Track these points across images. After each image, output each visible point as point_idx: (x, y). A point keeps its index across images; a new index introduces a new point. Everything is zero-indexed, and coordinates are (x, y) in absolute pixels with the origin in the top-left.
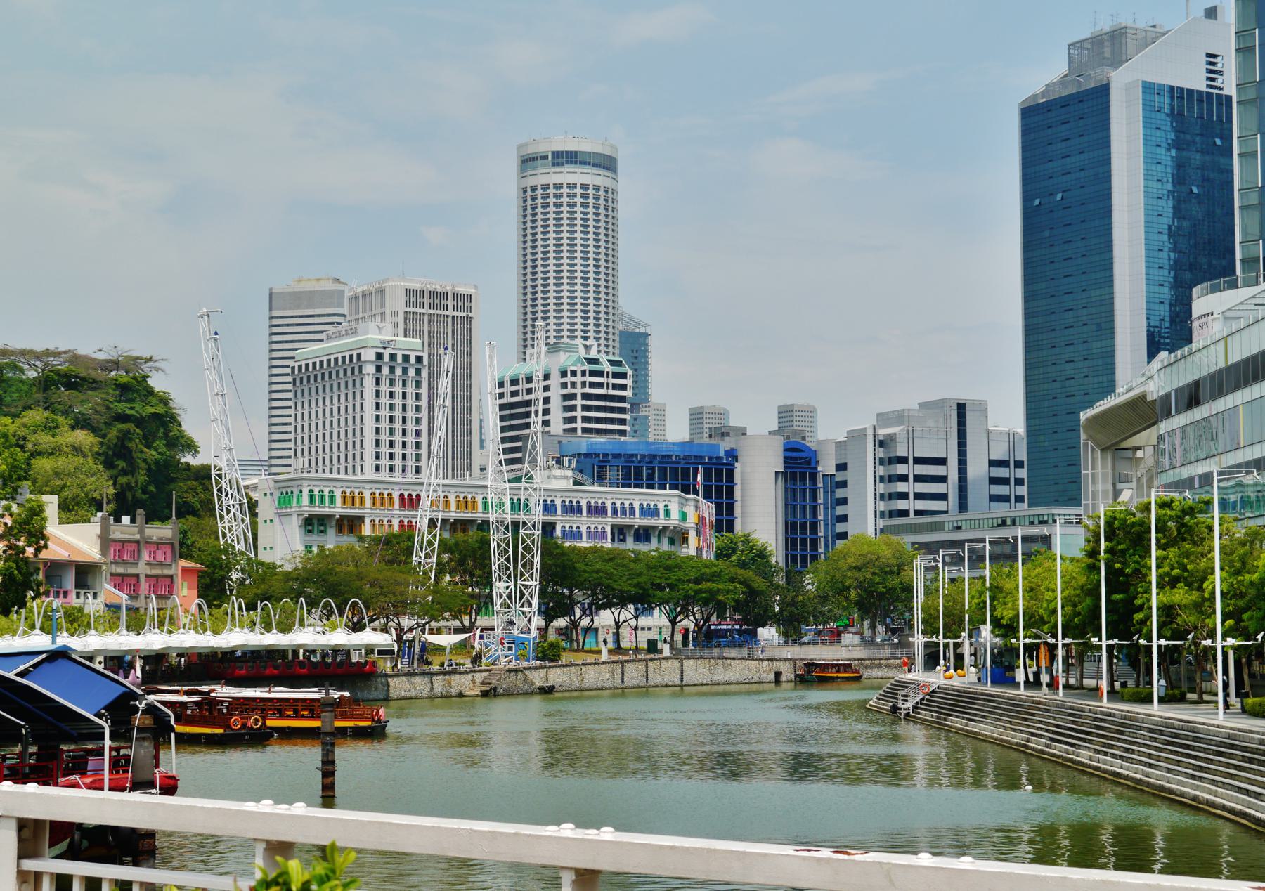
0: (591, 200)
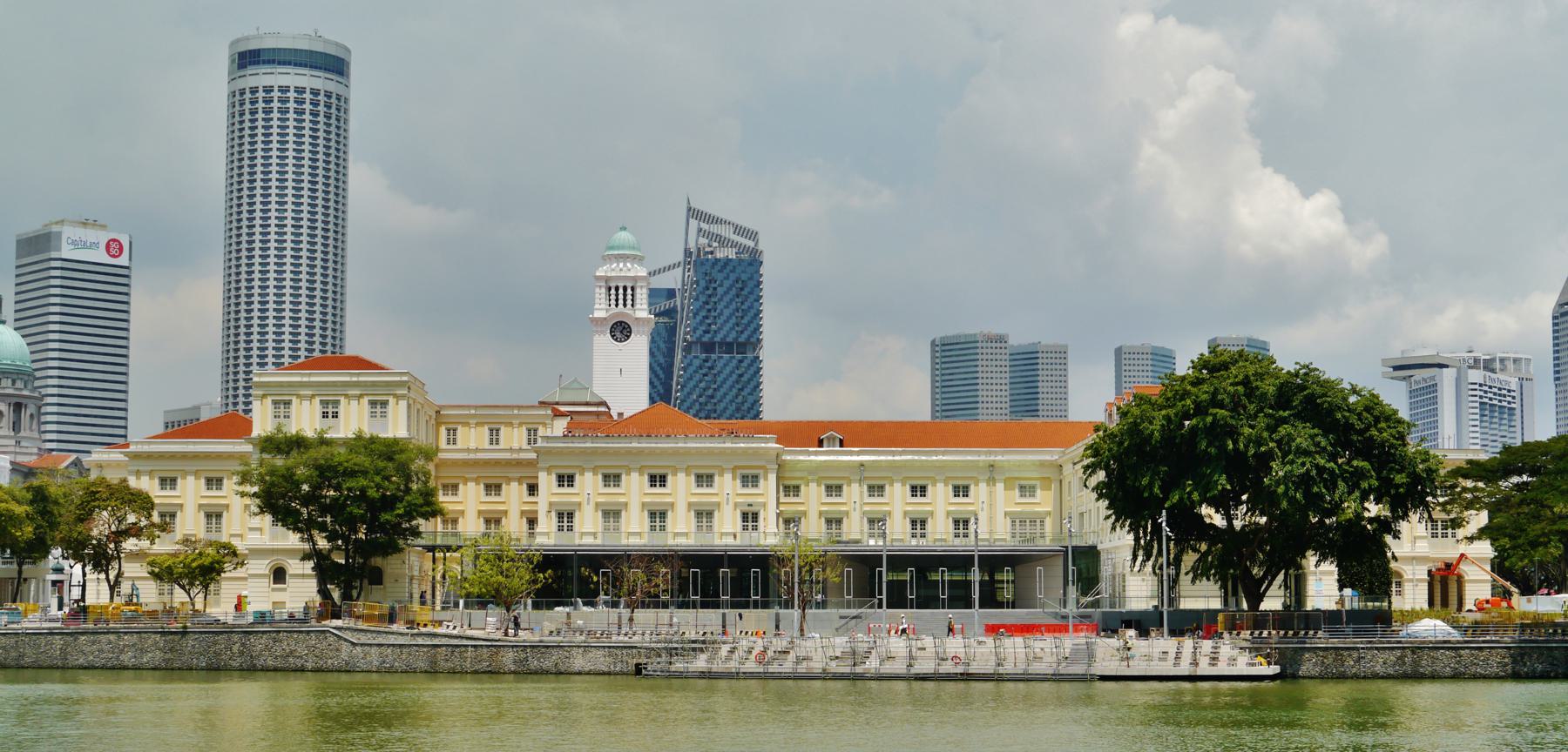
0: (321, 108)
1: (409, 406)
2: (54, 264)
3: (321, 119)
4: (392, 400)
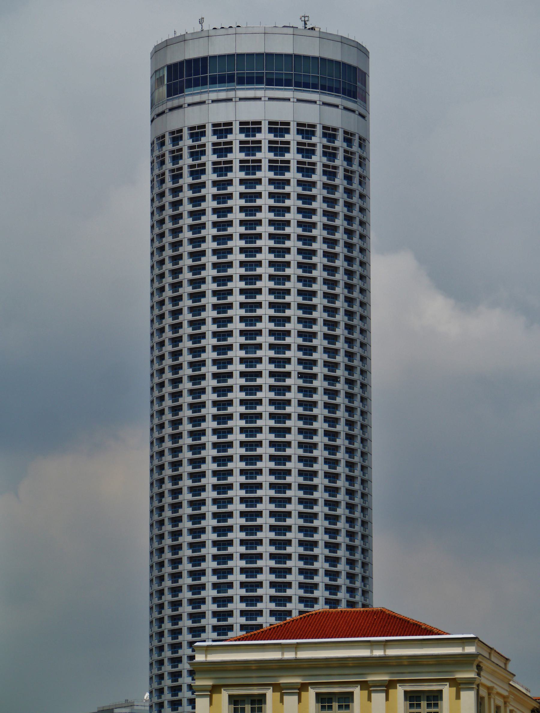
0: (318, 158)
1: (480, 701)
3: (318, 177)
4: (447, 691)
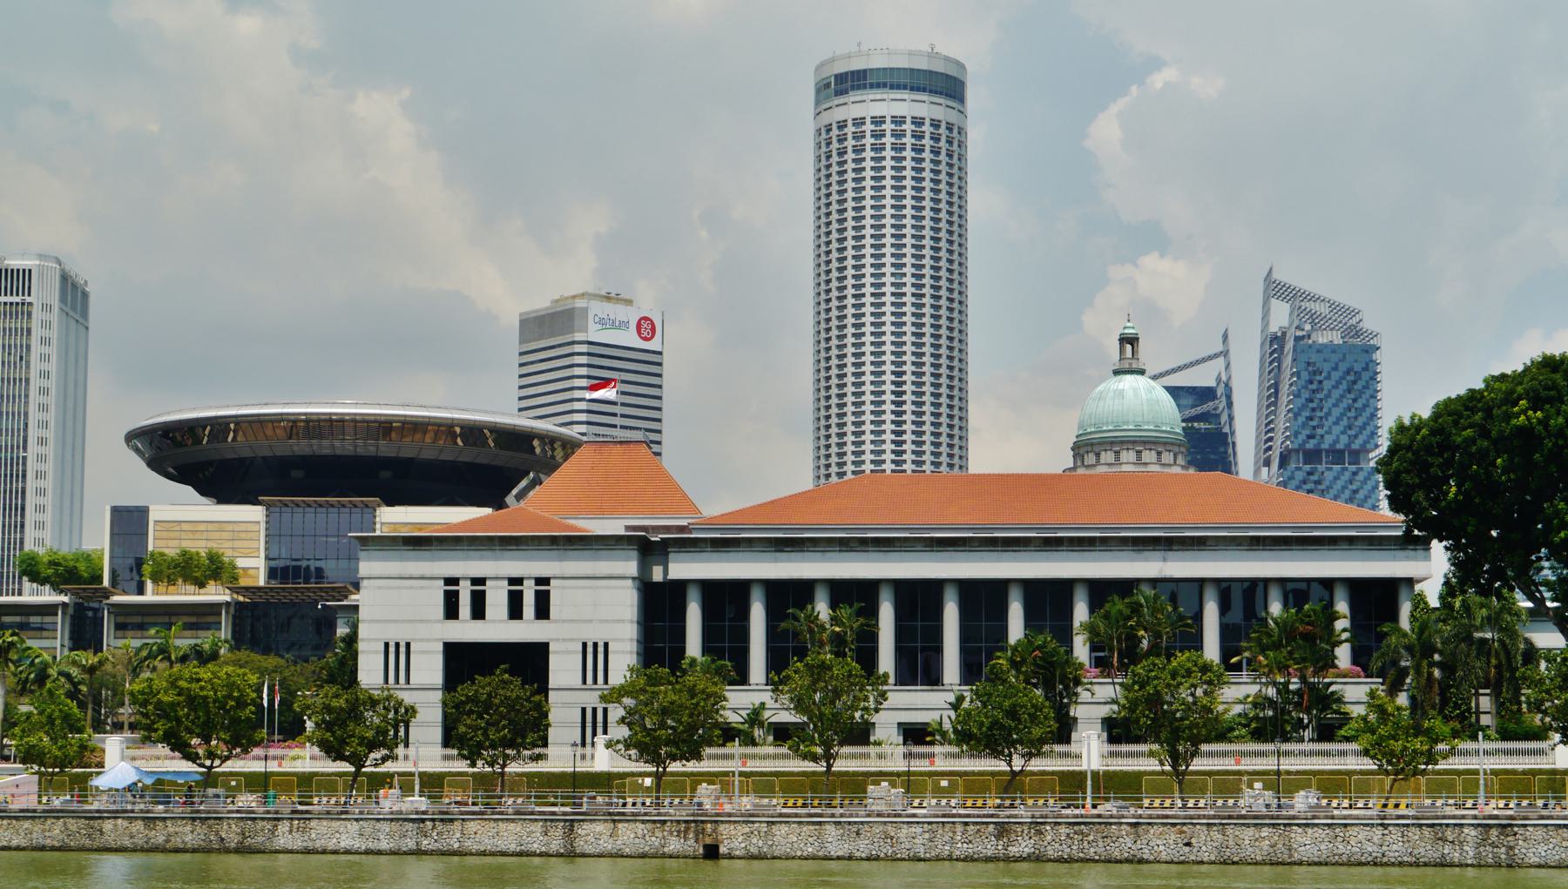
2: (578, 348)
3: (927, 155)
